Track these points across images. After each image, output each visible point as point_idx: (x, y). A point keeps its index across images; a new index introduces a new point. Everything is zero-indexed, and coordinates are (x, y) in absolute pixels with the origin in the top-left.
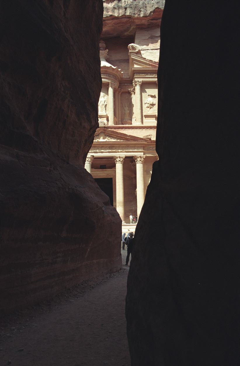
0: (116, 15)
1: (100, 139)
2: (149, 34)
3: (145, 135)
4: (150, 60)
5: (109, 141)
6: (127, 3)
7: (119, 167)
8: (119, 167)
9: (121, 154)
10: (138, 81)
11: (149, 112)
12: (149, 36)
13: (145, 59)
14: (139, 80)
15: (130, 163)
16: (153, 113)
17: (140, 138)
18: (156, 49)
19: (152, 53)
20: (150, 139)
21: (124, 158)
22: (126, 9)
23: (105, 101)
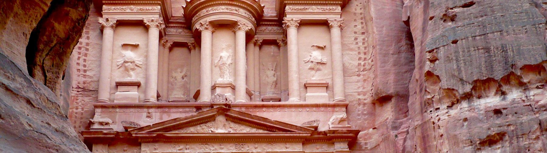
1: (217, 129)
3: (306, 121)
10: (292, 20)
11: (314, 78)
17: (296, 126)
20: (316, 128)
23: (228, 57)
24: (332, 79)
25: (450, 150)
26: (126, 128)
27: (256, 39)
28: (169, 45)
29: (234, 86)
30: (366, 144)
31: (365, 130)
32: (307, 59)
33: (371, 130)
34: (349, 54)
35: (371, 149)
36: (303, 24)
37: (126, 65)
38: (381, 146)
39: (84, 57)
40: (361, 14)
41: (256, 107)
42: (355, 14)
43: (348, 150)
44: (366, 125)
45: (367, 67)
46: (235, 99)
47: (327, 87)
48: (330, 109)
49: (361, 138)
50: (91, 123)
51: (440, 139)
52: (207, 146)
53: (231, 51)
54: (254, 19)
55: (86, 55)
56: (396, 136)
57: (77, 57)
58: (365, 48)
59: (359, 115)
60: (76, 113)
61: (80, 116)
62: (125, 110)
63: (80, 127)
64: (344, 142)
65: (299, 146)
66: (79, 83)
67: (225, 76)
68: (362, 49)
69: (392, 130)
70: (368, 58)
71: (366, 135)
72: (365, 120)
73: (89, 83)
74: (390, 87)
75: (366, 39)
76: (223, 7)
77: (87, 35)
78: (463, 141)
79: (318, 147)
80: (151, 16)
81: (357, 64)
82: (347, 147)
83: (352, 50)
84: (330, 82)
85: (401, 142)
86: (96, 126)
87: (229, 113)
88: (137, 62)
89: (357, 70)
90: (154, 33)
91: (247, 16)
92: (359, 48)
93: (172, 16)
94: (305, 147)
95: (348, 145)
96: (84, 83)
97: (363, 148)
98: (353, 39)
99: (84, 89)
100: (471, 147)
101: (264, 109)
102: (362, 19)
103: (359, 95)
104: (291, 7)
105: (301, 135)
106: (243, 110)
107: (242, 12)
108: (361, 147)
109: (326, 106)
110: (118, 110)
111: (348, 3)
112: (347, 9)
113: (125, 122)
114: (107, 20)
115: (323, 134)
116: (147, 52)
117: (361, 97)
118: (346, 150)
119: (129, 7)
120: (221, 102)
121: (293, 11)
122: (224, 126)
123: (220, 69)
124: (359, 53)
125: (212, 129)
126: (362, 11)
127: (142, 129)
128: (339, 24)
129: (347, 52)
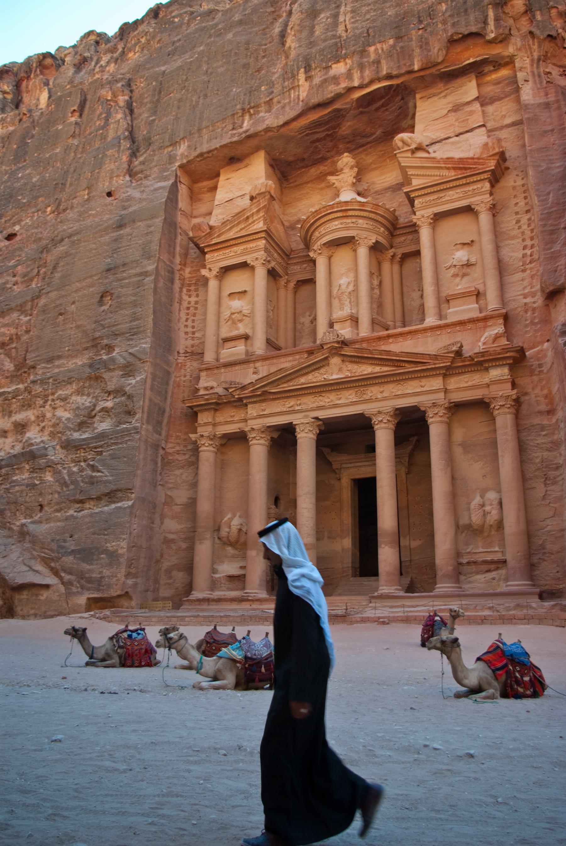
0: (356, 84)
2: (449, 103)
4: (448, 158)
5: (353, 375)
6: (380, 52)
7: (384, 438)
8: (384, 438)
10: (423, 217)
11: (459, 287)
12: (450, 107)
13: (434, 158)
14: (423, 214)
16: (469, 287)
17: (429, 355)
18: (467, 132)
19: (458, 142)
20: (459, 353)
21: (392, 413)
22: (377, 62)
23: (349, 283)
24: (484, 283)
26: (226, 389)
27: (392, 254)
28: (292, 285)
29: (357, 319)
30: (540, 366)
32: (449, 264)
34: (509, 245)
35: (548, 372)
36: (438, 217)
37: (233, 316)
39: (193, 318)
40: (523, 185)
41: (380, 338)
42: (514, 188)
43: (509, 377)
44: (538, 339)
45: (536, 256)
46: (358, 334)
47: (478, 295)
48: (480, 324)
49: (532, 358)
50: (198, 390)
52: (321, 398)
53: (352, 275)
54: (382, 229)
55: (194, 315)
57: (185, 319)
58: (532, 231)
59: (526, 326)
60: (184, 381)
61: (188, 384)
62: (229, 369)
63: (189, 396)
65: (438, 381)
66: (186, 347)
67: (345, 308)
68: (528, 233)
70: (536, 244)
72: (536, 331)
73: (197, 346)
74: (561, 275)
75: (533, 218)
76: (336, 223)
77: (195, 293)
80: (256, 254)
81: (521, 256)
83: (513, 238)
84: (481, 289)
86: (202, 392)
87: (342, 353)
88: (246, 312)
89: (521, 264)
90: (261, 273)
91: (371, 227)
92: (523, 233)
93: (292, 251)
95: (511, 370)
96: (192, 346)
97: (536, 373)
98: (514, 222)
99: (192, 353)
101: (391, 340)
102: (524, 192)
103: (525, 298)
104: (420, 200)
105: (437, 366)
106: (364, 345)
107: (361, 221)
109: (474, 321)
110: (223, 370)
111: (503, 174)
112: (502, 183)
113: (226, 382)
114: (210, 270)
115: (469, 361)
116: (253, 298)
117: (528, 300)
118: (505, 377)
119: (232, 249)
120: (332, 340)
121: (424, 204)
122: (340, 370)
123: (340, 300)
124: (524, 240)
125: (325, 376)
126: (523, 182)
127: (243, 388)
128: (488, 206)
129: (507, 242)
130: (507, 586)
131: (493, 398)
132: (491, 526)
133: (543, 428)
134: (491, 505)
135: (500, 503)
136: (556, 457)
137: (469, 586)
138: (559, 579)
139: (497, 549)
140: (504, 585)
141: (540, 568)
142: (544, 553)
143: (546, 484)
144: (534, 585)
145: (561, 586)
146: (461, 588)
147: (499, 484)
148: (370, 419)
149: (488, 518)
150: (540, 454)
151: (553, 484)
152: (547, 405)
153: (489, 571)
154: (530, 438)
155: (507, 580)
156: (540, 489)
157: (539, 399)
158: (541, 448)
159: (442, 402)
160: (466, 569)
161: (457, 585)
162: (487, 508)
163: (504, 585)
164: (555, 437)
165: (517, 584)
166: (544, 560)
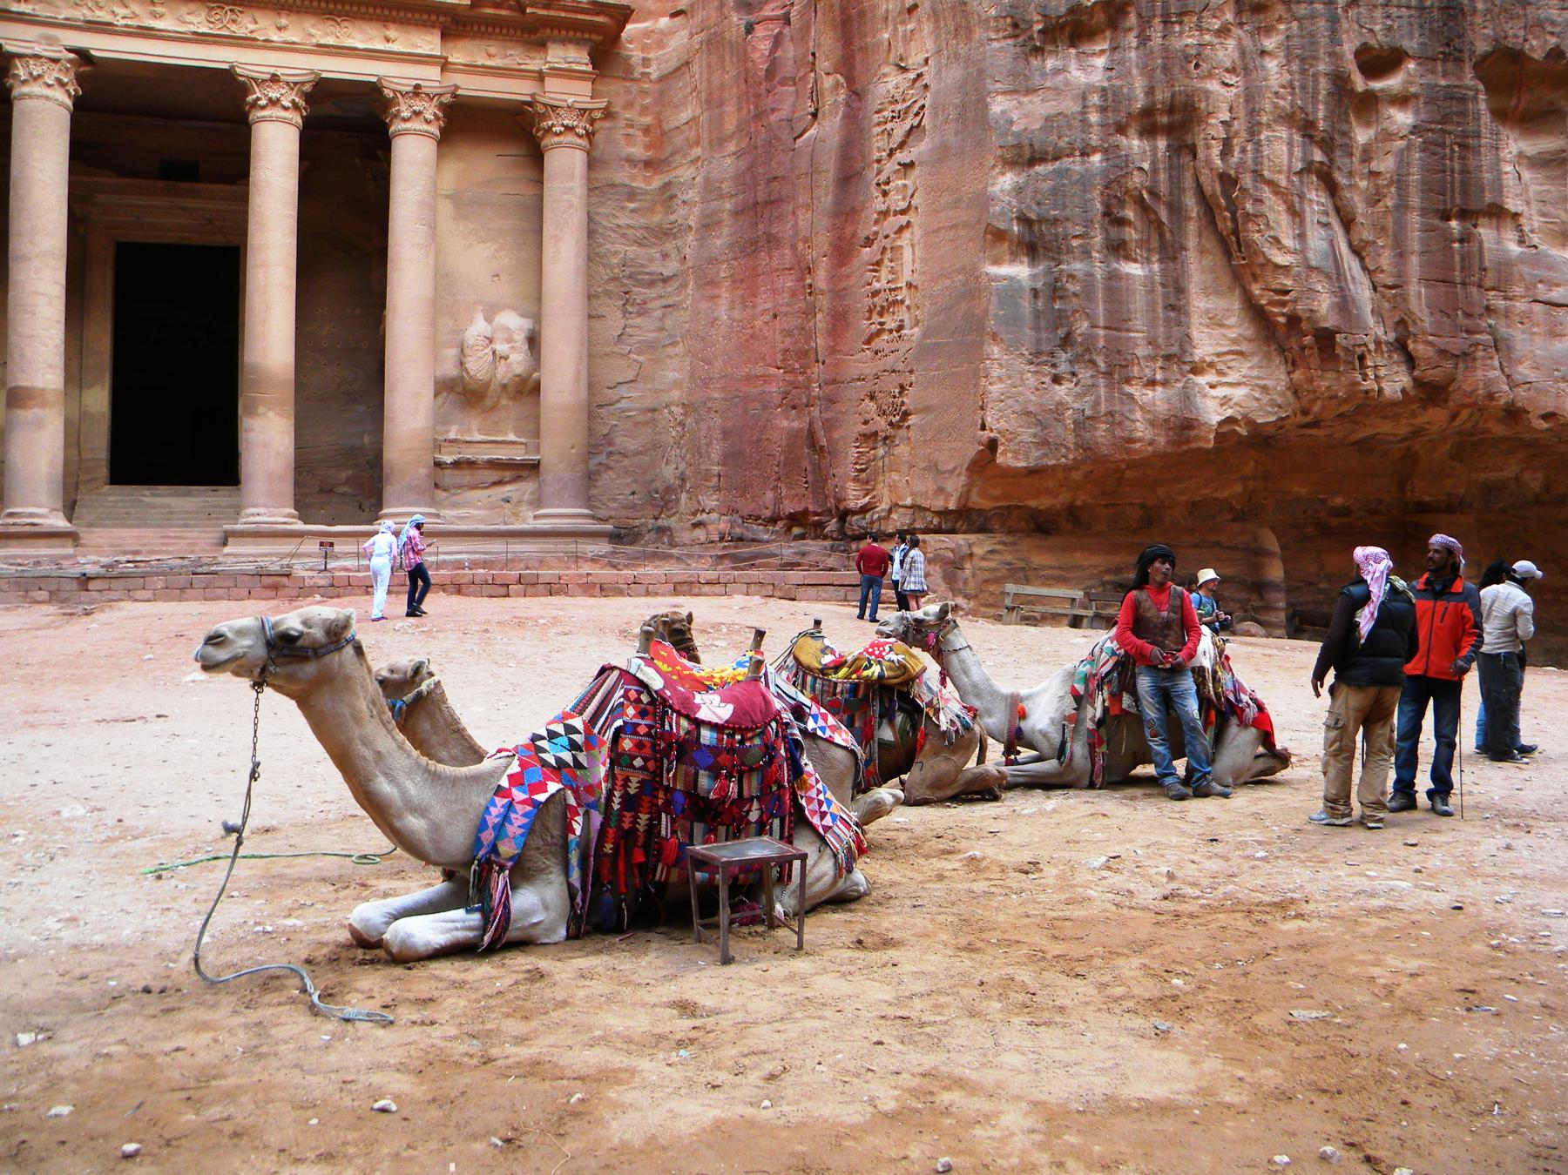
9: (283, 58)
15: (357, 160)
21: (307, 88)
25: (938, 52)
30: (646, 62)
31: (645, 20)
33: (664, 22)
35: (661, 79)
38: (695, 68)
43: (590, 68)
49: (631, 42)
51: (903, 23)
56: (750, 29)
64: (577, 42)
65: (429, 38)
69: (738, 11)
71: (647, 33)
78: (987, 20)
79: (493, 50)
82: (586, 59)
85: (764, 47)
94: (450, 45)
97: (636, 75)
100: (1010, 42)
108: (629, 69)
118: (584, 68)
130: (536, 517)
131: (552, 107)
132: (504, 386)
133: (632, 195)
134: (509, 340)
135: (533, 341)
136: (651, 260)
137: (454, 512)
138: (634, 506)
139: (512, 437)
140: (531, 514)
141: (600, 483)
142: (611, 453)
143: (625, 312)
144: (592, 517)
145: (637, 522)
146: (438, 516)
147: (539, 298)
148: (244, 89)
149: (502, 369)
150: (618, 247)
151: (639, 315)
152: (648, 147)
153: (499, 483)
154: (601, 210)
155: (537, 502)
156: (614, 321)
157: (631, 131)
158: (624, 235)
159: (428, 86)
160: (449, 477)
161: (433, 511)
162: (502, 348)
163: (531, 514)
164: (656, 219)
165: (564, 513)
166: (609, 468)
